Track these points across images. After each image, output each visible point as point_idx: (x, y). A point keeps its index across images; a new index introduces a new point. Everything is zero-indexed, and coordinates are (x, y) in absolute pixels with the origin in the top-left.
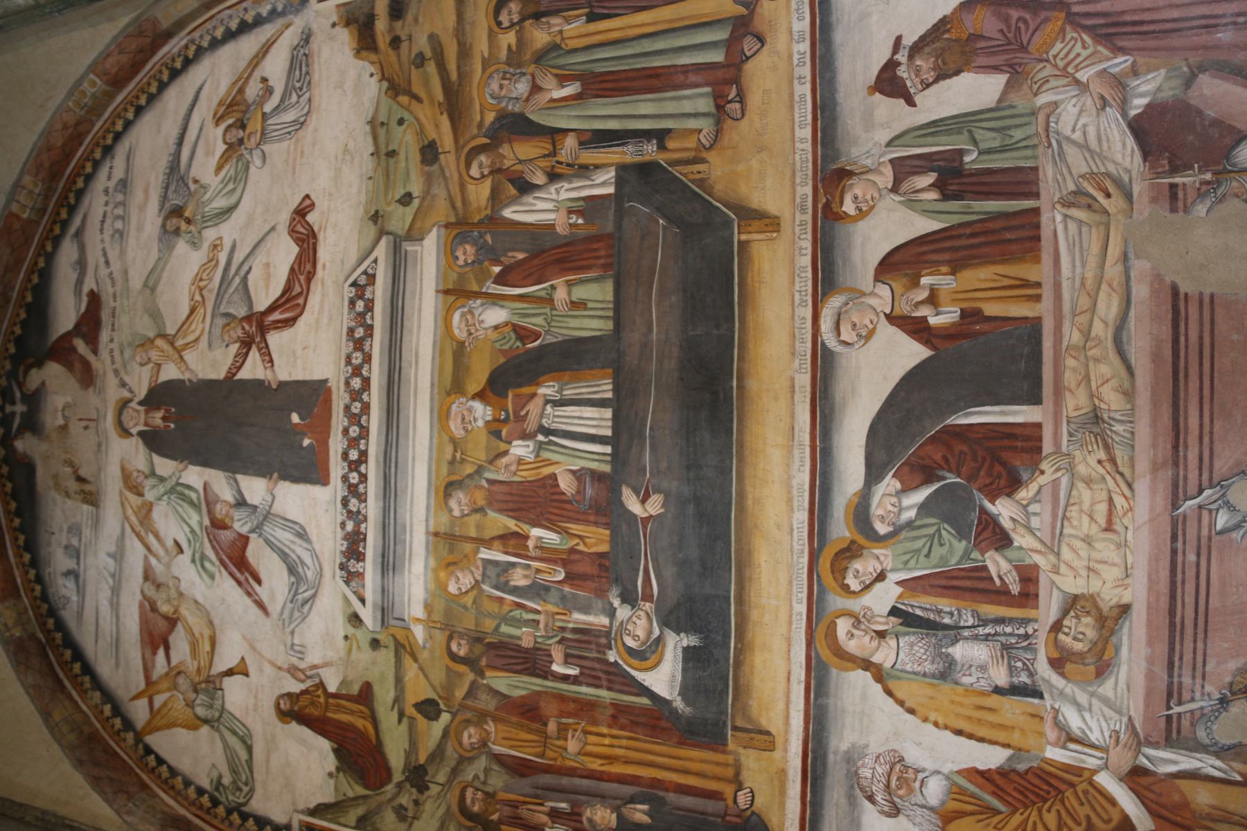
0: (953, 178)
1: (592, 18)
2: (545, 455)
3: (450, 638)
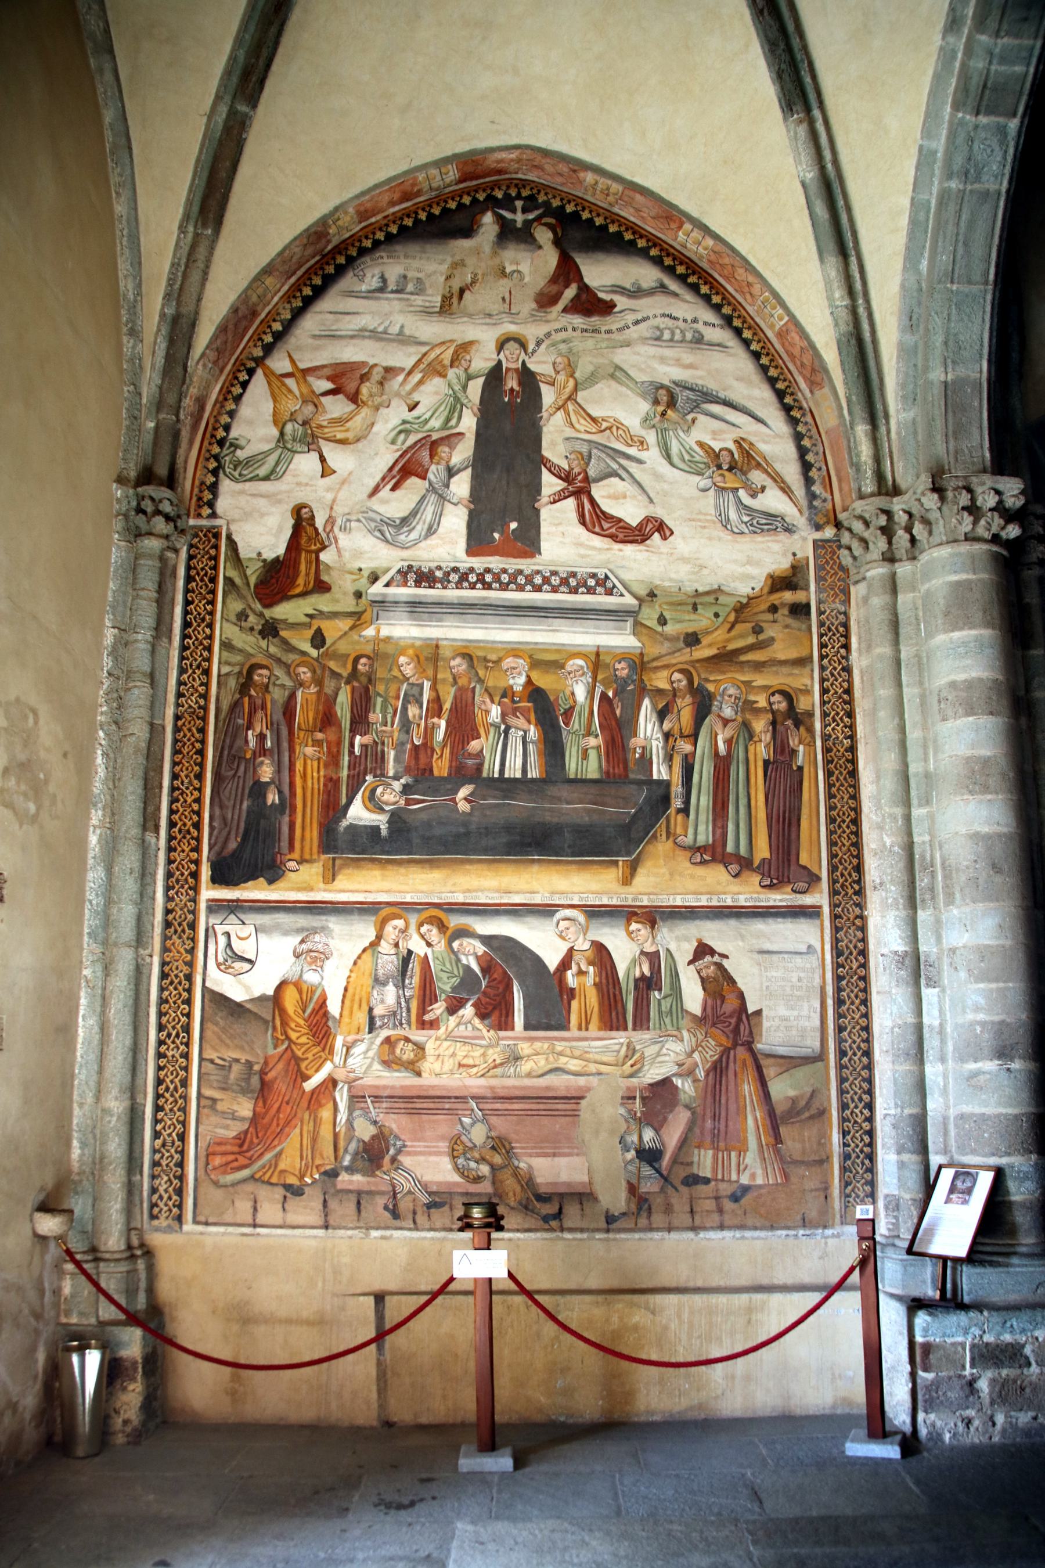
0: (647, 984)
1: (766, 763)
2: (492, 730)
3: (369, 657)
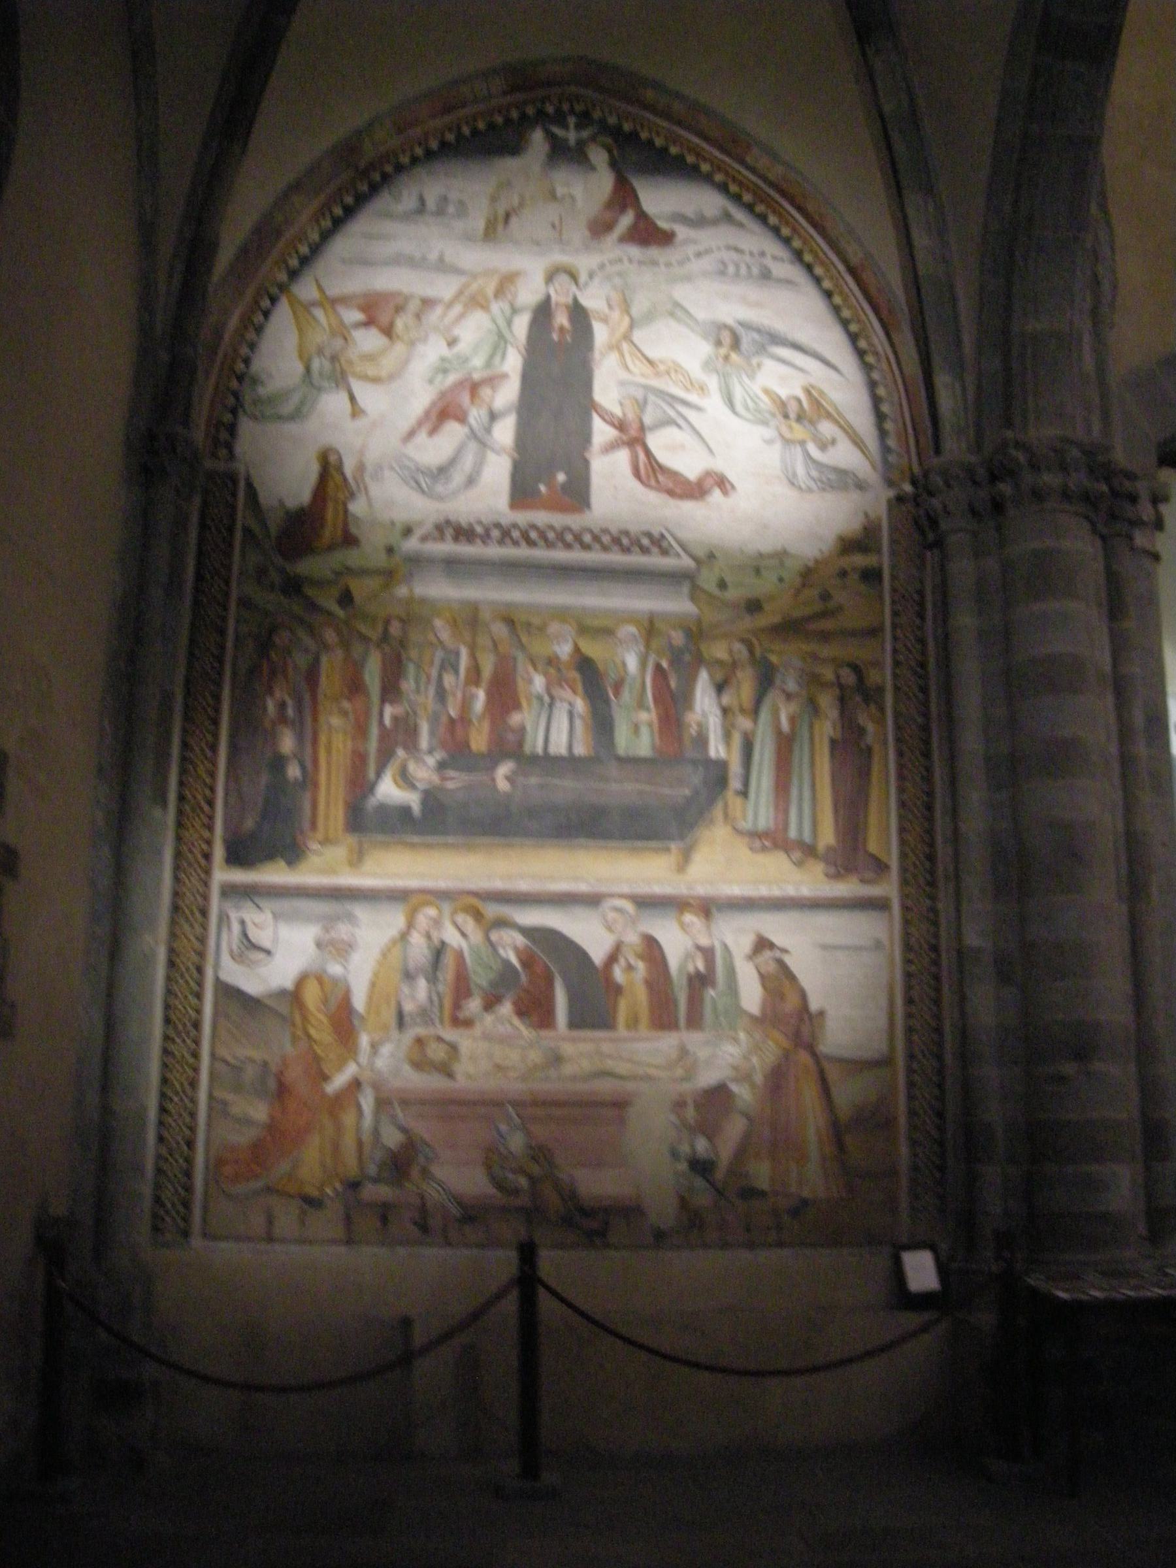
0: (700, 982)
2: (535, 702)
